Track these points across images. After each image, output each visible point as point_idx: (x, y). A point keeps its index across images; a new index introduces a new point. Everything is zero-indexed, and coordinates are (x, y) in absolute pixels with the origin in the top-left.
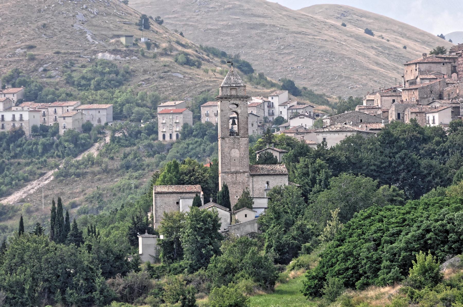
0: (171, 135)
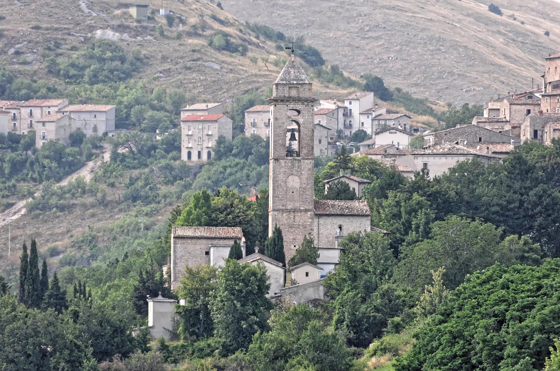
0: (199, 152)
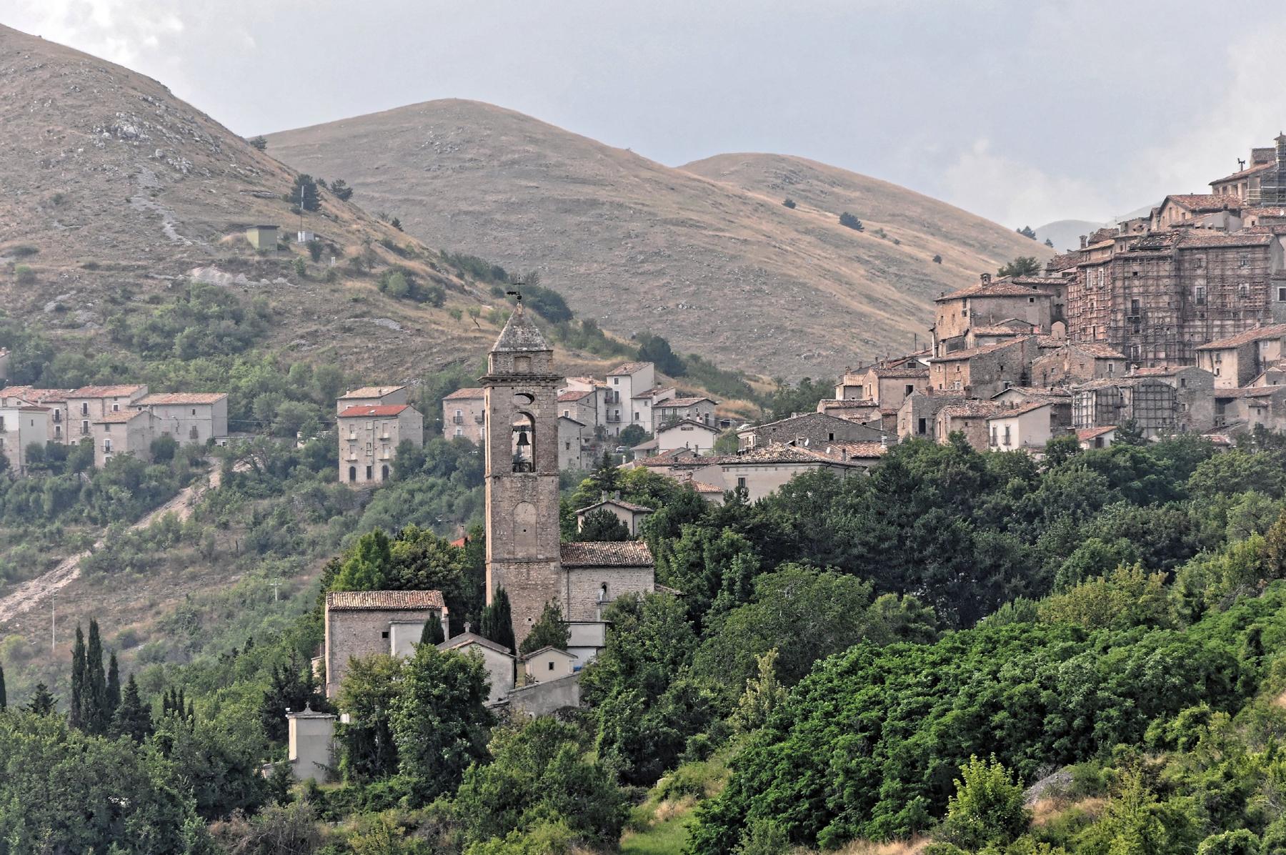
0: (369, 469)
